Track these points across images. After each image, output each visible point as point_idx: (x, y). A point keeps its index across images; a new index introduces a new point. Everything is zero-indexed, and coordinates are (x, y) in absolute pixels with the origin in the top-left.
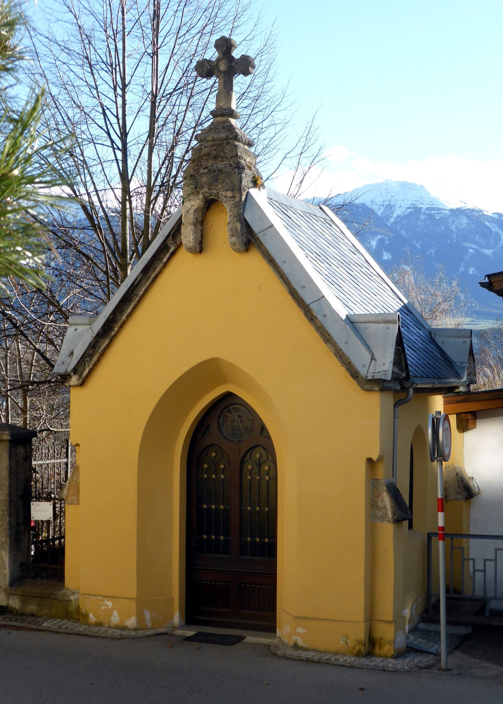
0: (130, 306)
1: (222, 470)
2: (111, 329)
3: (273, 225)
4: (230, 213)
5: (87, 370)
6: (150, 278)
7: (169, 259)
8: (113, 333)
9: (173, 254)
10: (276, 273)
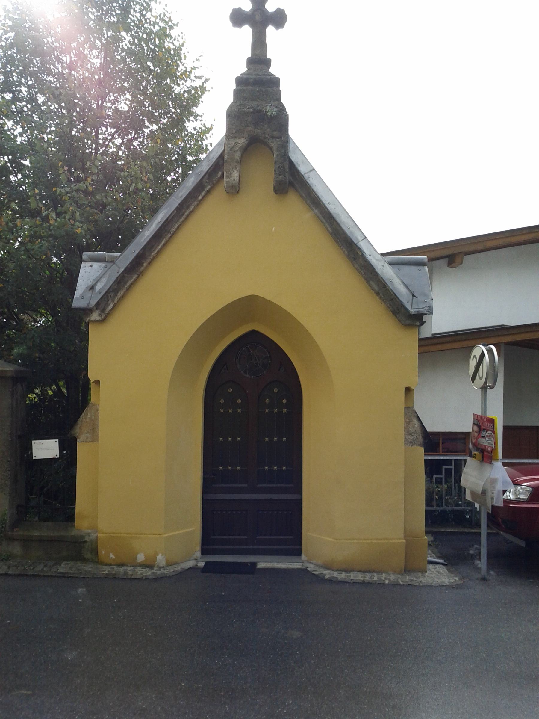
0: (161, 242)
1: (253, 392)
2: (141, 264)
3: (314, 169)
4: (277, 153)
5: (112, 305)
6: (183, 215)
7: (204, 197)
8: (142, 268)
9: (208, 192)
10: (331, 208)
